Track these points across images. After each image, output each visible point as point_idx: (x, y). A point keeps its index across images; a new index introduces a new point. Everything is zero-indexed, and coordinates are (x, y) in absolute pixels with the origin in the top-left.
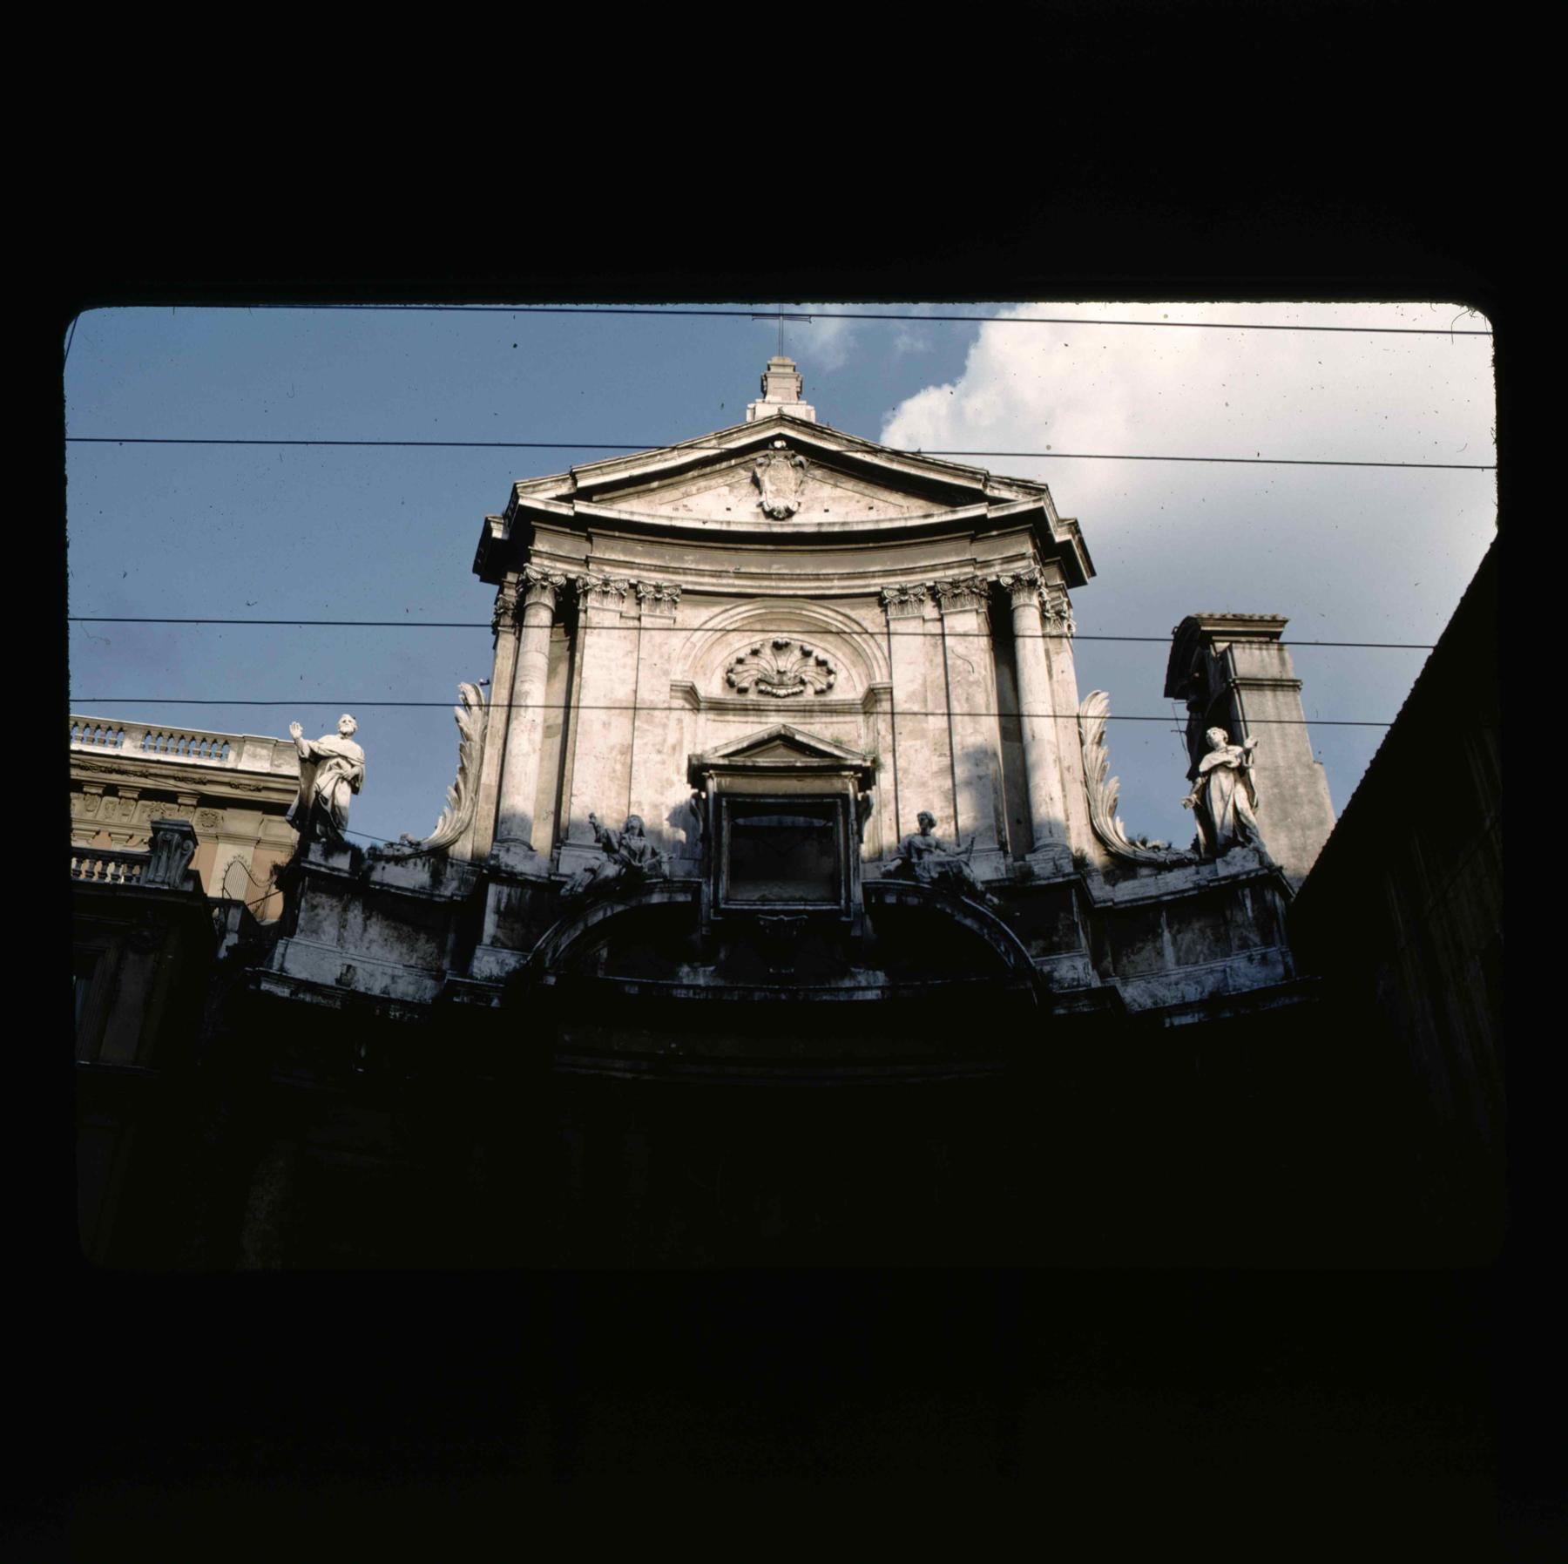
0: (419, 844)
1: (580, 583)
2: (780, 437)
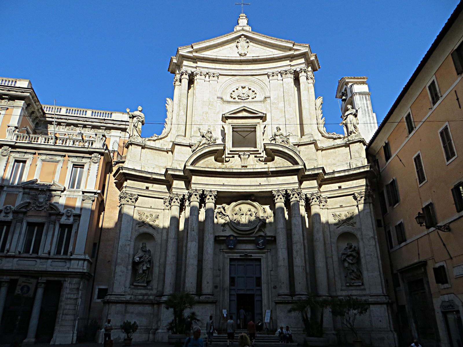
1: (194, 73)
2: (243, 35)
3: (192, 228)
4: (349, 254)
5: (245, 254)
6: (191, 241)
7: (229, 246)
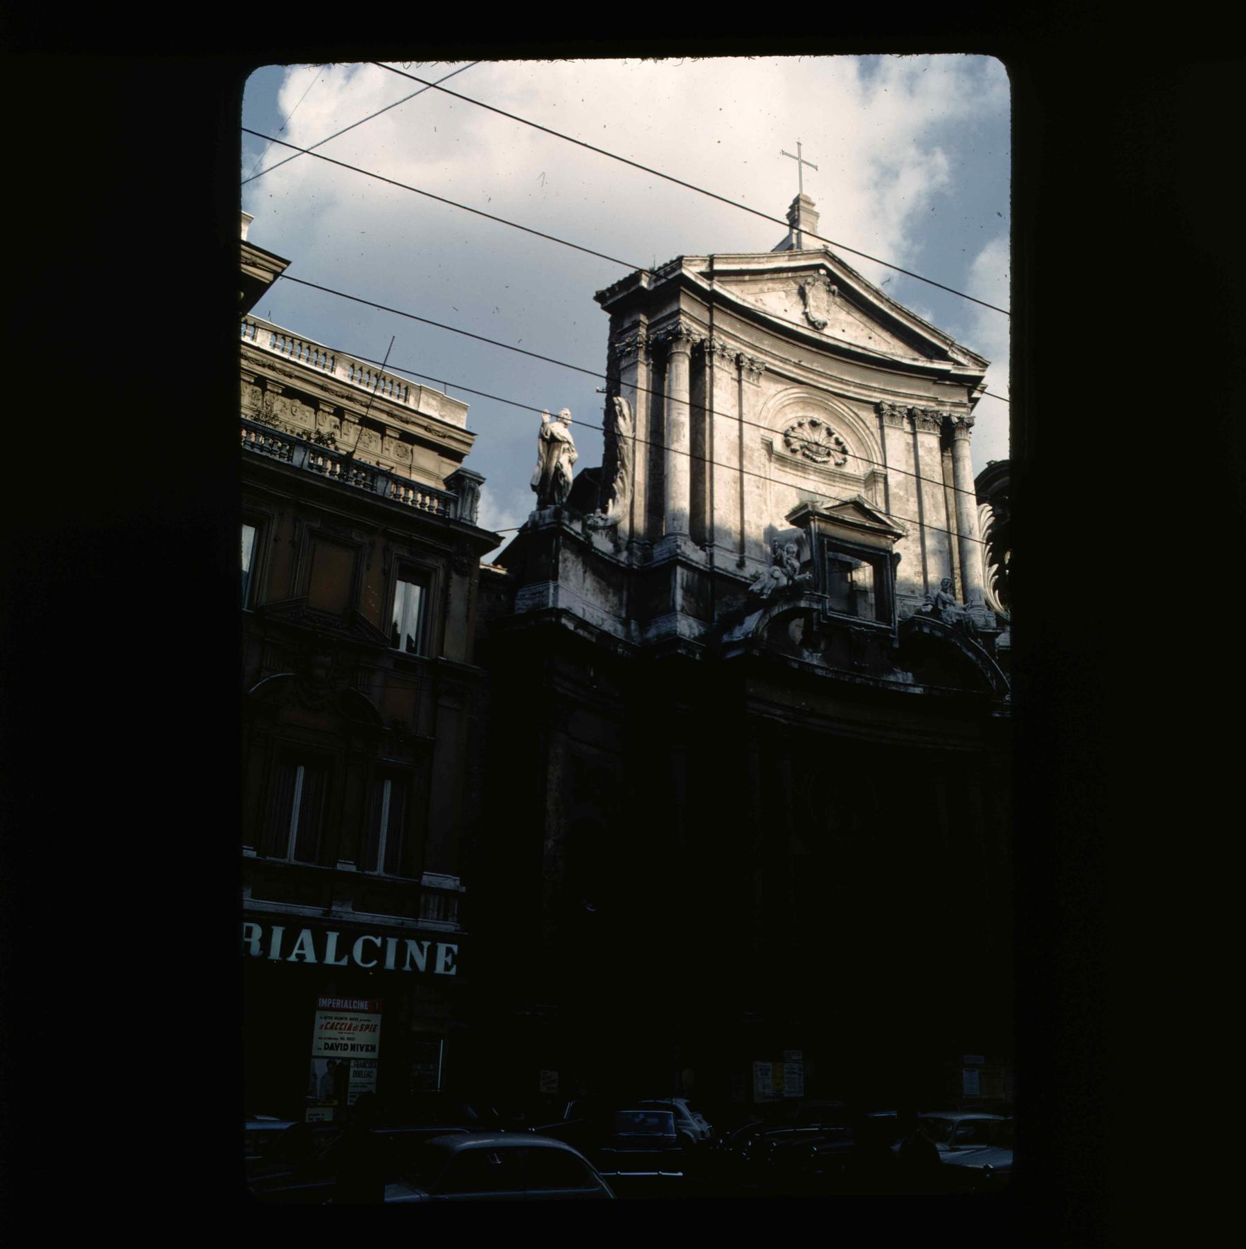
1: (707, 344)
2: (822, 266)
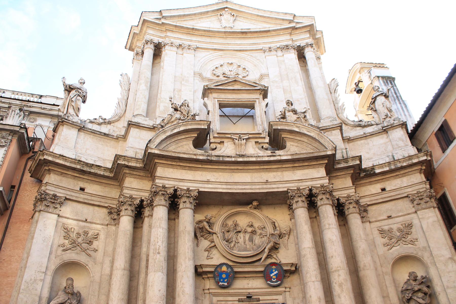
0: (105, 119)
2: (227, 8)
3: (156, 249)
4: (416, 289)
5: (248, 297)
6: (155, 271)
7: (220, 283)
